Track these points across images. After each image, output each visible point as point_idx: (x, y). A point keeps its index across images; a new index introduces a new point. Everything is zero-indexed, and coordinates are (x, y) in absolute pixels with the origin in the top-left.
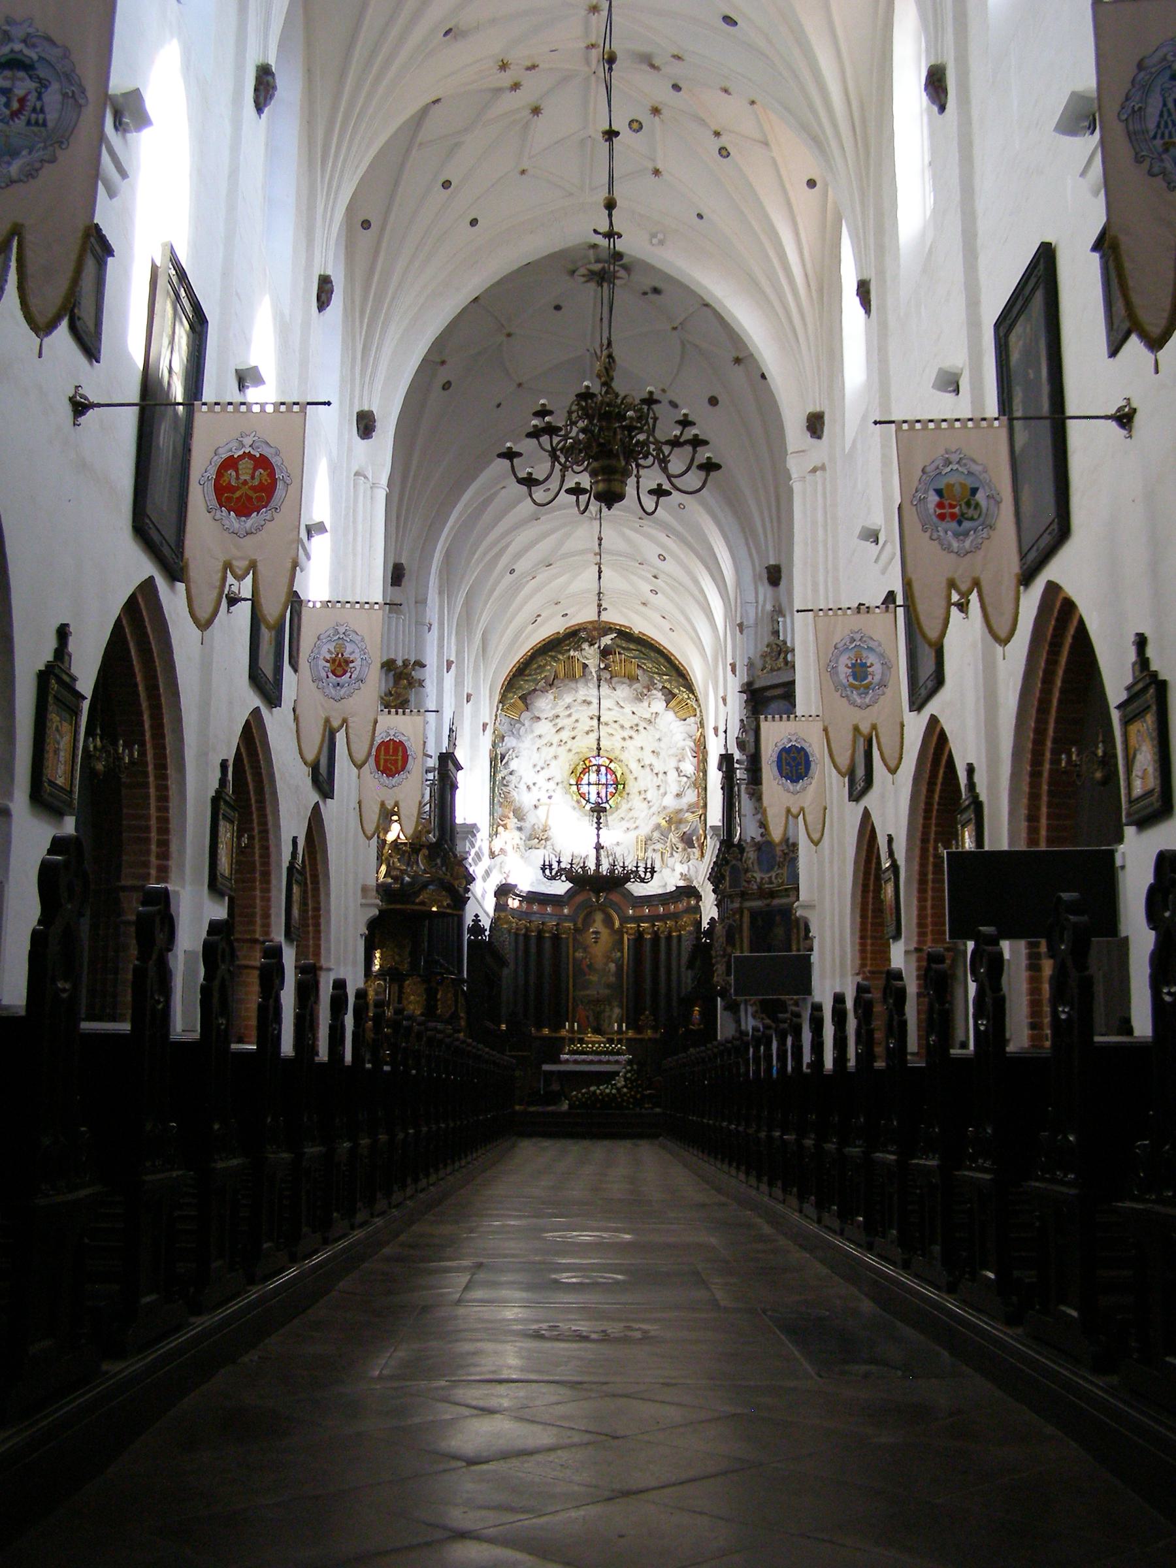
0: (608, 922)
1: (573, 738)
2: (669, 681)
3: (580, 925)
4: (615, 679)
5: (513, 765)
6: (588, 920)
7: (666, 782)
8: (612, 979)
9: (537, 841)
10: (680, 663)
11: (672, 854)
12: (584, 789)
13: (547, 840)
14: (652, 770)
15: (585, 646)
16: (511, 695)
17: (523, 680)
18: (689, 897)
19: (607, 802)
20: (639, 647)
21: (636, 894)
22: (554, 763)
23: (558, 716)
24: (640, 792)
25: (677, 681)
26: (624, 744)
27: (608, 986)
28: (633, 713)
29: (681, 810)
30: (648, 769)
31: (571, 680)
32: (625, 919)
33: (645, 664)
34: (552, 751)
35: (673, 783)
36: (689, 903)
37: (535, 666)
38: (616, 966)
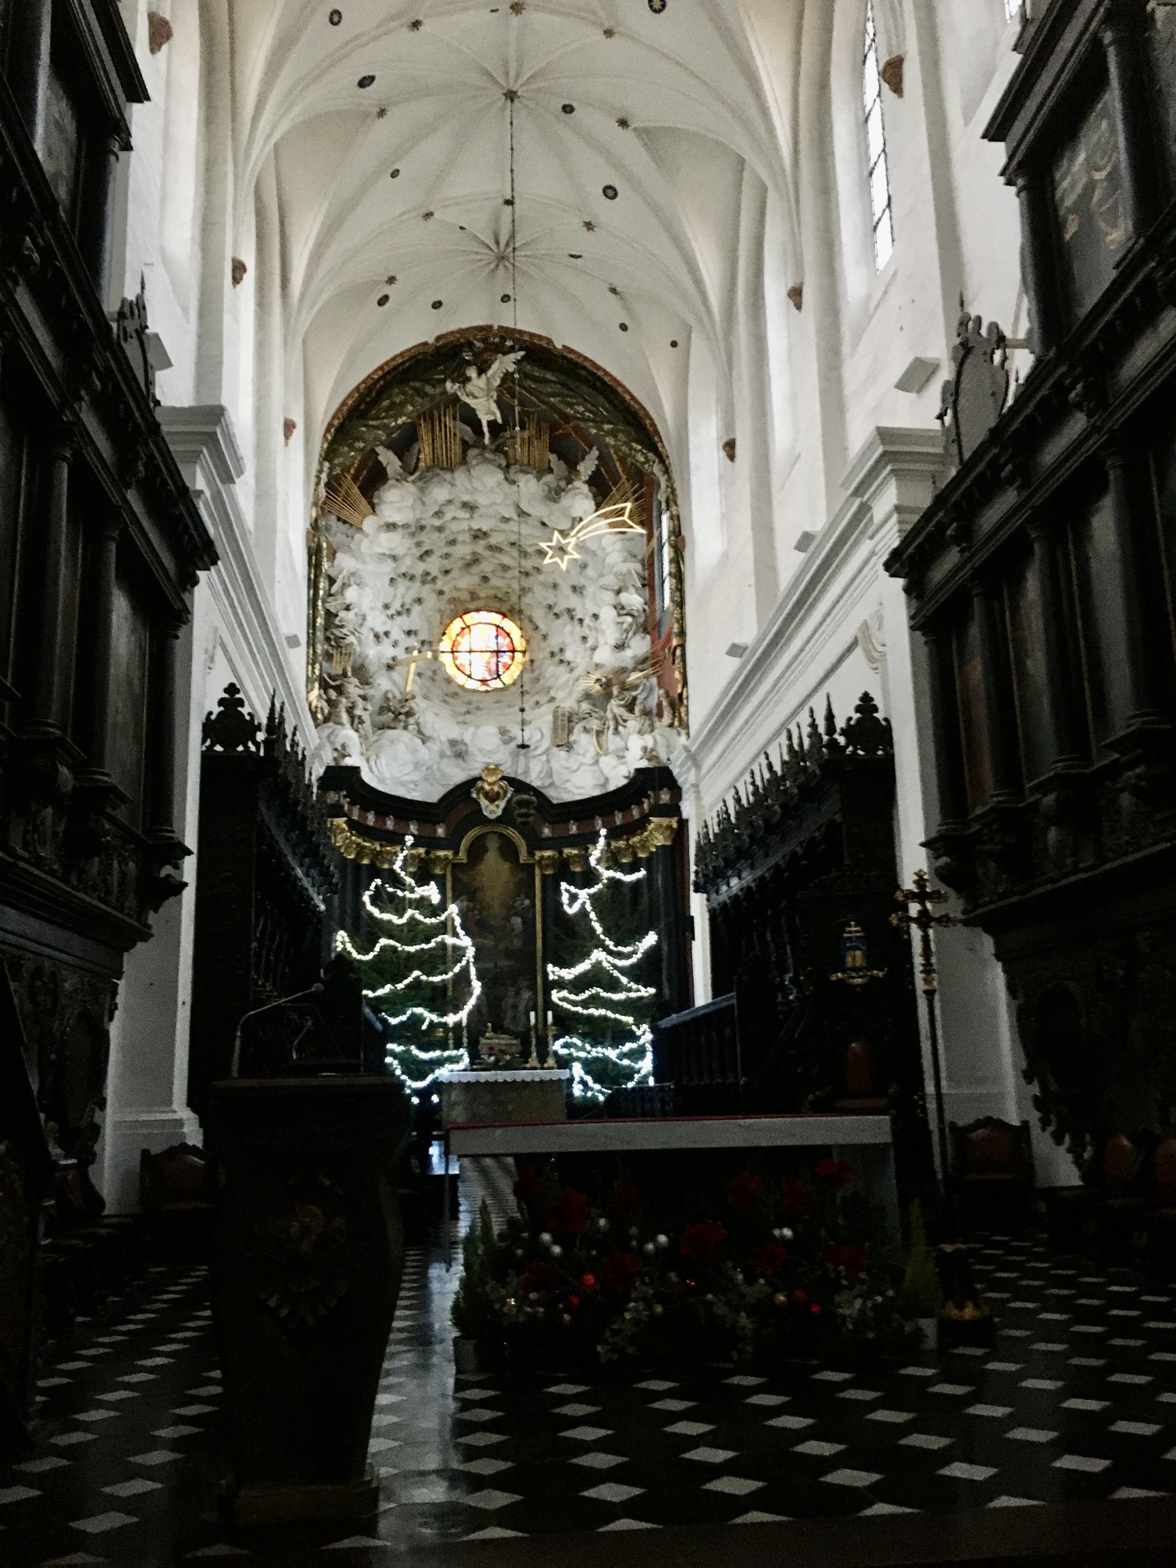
0: (508, 851)
1: (447, 572)
2: (613, 434)
3: (463, 856)
4: (513, 469)
5: (351, 595)
6: (477, 851)
7: (597, 630)
8: (517, 943)
9: (391, 715)
10: (633, 398)
11: (616, 729)
12: (463, 659)
13: (409, 714)
14: (572, 618)
15: (472, 372)
16: (346, 449)
17: (366, 426)
18: (657, 789)
19: (499, 676)
20: (563, 378)
21: (555, 802)
22: (416, 609)
23: (422, 528)
24: (552, 654)
25: (628, 434)
26: (526, 582)
27: (509, 954)
28: (544, 524)
29: (623, 671)
30: (565, 618)
31: (443, 469)
32: (536, 843)
33: (571, 405)
34: (416, 589)
35: (609, 628)
36: (658, 798)
37: (386, 403)
38: (524, 923)
